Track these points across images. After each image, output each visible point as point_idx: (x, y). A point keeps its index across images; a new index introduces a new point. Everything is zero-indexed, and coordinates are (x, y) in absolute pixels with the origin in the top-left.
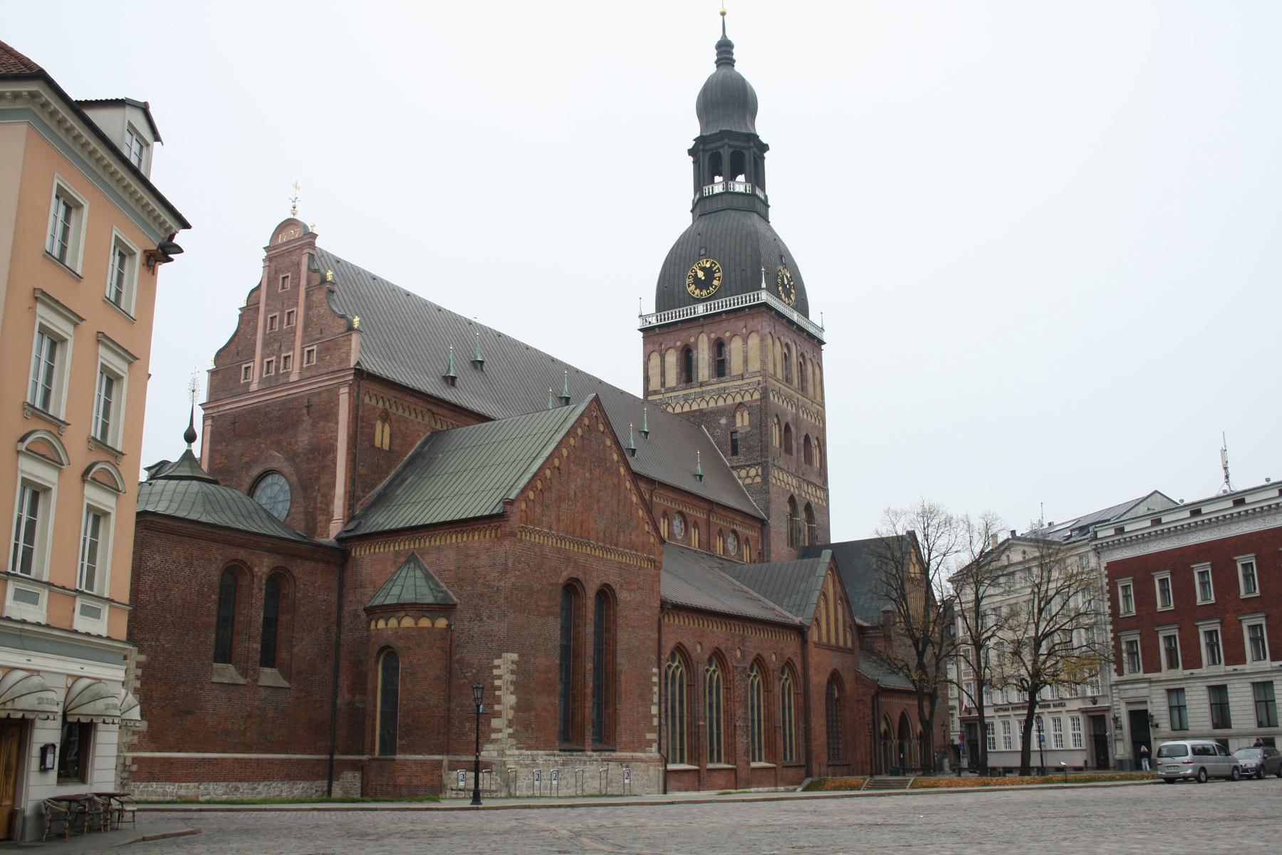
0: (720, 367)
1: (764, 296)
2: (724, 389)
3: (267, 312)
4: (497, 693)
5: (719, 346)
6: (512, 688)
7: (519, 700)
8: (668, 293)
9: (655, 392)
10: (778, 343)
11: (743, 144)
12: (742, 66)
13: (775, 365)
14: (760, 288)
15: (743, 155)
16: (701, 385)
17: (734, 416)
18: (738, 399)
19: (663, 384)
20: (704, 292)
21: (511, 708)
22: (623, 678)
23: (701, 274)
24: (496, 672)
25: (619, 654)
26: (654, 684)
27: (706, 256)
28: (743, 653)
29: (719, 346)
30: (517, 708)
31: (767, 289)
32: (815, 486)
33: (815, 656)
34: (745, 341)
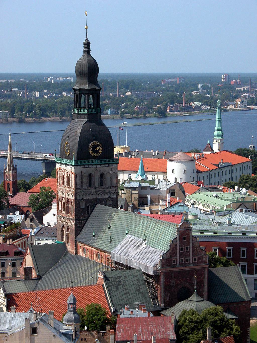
0: (102, 184)
3: (180, 246)
4: (249, 335)
5: (102, 175)
9: (79, 189)
16: (96, 188)
19: (82, 186)
20: (93, 154)
23: (98, 148)
24: (248, 331)
27: (96, 140)
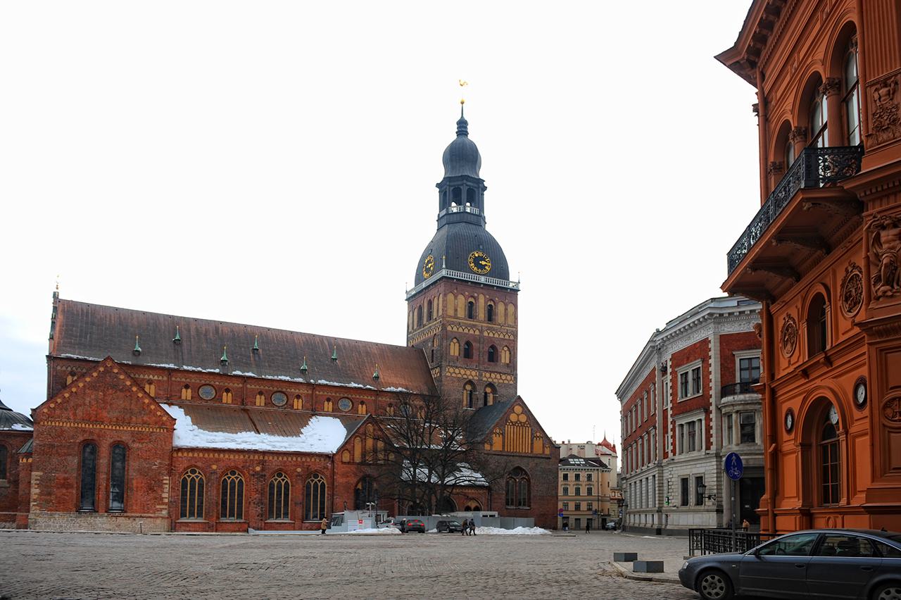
1: (444, 273)
2: (430, 327)
6: (36, 486)
7: (42, 491)
8: (419, 279)
10: (461, 298)
11: (460, 183)
12: (473, 135)
13: (456, 310)
14: (441, 268)
15: (461, 190)
17: (433, 342)
18: (435, 332)
21: (35, 494)
22: (134, 482)
25: (130, 471)
26: (166, 484)
28: (263, 470)
29: (430, 303)
30: (41, 494)
31: (447, 268)
32: (500, 373)
33: (340, 469)
34: (438, 299)
